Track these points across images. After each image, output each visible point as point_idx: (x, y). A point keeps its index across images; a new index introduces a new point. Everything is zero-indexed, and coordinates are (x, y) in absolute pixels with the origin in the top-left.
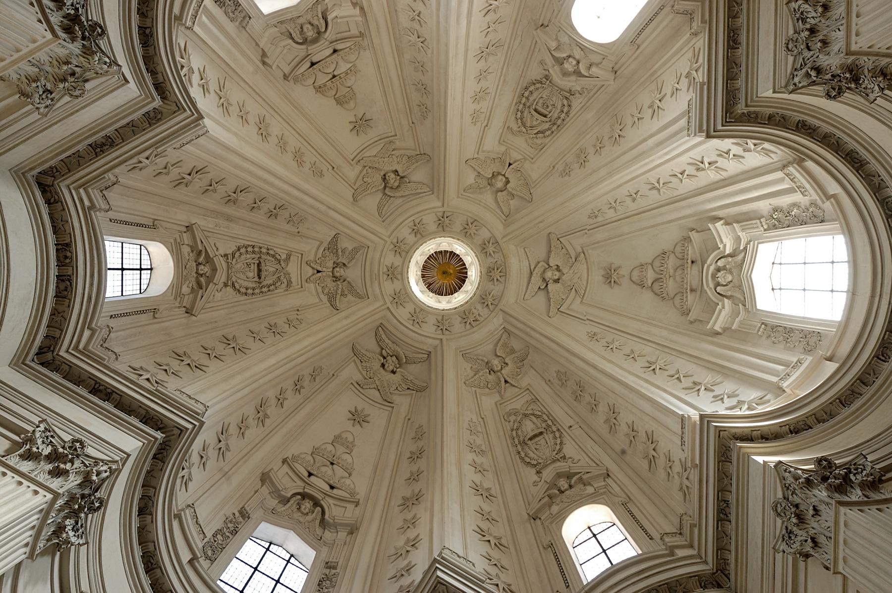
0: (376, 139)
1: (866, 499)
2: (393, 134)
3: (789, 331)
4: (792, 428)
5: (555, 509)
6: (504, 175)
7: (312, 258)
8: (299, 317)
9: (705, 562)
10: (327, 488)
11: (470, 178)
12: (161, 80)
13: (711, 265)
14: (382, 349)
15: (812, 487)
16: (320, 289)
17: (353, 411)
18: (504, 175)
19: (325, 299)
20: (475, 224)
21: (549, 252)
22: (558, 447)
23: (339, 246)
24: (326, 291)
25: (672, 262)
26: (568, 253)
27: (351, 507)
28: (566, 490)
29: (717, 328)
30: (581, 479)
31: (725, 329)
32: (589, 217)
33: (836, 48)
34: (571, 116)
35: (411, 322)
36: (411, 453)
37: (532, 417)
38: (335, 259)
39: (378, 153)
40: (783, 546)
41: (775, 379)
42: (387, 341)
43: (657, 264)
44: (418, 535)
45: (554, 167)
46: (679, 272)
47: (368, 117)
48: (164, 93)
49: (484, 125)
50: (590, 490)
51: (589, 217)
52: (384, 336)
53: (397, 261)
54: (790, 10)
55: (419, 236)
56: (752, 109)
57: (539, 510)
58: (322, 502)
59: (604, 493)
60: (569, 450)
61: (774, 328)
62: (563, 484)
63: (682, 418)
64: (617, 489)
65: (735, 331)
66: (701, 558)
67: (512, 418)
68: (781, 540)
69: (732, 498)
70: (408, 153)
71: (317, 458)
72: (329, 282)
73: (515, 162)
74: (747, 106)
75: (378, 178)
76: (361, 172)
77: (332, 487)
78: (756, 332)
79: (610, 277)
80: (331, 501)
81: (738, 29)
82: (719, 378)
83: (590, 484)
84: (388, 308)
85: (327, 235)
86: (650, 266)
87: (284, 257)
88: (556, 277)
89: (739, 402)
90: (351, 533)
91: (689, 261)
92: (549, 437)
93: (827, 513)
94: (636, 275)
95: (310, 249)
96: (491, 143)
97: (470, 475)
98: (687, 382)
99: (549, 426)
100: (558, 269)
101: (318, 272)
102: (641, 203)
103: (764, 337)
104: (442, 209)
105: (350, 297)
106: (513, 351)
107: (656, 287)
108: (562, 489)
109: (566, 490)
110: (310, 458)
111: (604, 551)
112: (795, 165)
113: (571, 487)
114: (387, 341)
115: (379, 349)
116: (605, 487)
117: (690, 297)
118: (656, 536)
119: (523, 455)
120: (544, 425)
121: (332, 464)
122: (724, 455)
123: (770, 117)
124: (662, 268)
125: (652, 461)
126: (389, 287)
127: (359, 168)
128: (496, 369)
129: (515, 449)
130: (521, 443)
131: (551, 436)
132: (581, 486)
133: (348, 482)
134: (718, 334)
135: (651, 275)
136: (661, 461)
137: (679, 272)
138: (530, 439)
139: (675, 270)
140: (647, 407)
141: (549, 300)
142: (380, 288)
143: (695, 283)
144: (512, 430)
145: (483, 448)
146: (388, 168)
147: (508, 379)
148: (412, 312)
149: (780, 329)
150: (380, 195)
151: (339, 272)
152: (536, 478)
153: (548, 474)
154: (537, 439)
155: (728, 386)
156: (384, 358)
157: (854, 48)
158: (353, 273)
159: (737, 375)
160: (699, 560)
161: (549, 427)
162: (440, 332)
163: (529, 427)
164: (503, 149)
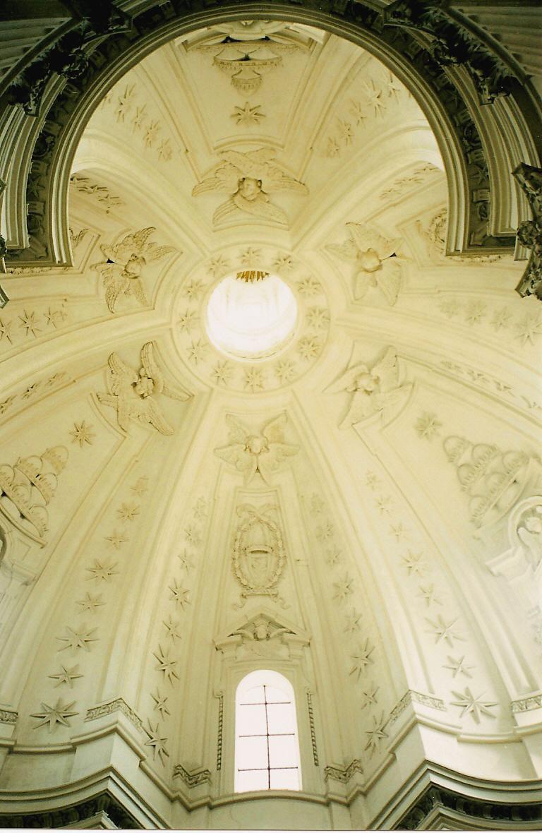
0: (257, 137)
2: (280, 143)
5: (242, 652)
6: (380, 261)
7: (107, 240)
8: (64, 310)
10: (15, 515)
11: (341, 239)
12: (39, 210)
13: (529, 503)
14: (143, 367)
16: (102, 278)
17: (79, 425)
18: (380, 261)
19: (103, 291)
20: (315, 286)
21: (380, 359)
22: (275, 579)
23: (148, 241)
24: (109, 283)
25: (494, 463)
26: (397, 374)
27: (36, 547)
28: (262, 639)
29: (494, 570)
31: (500, 574)
32: (442, 363)
34: (493, 264)
35: (189, 354)
36: (123, 505)
37: (266, 526)
38: (136, 252)
39: (250, 152)
42: (152, 361)
43: (479, 451)
44: (94, 631)
45: (439, 291)
46: (494, 479)
47: (260, 111)
48: (36, 227)
49: (393, 203)
50: (284, 652)
51: (442, 363)
52: (150, 356)
53: (207, 279)
55: (246, 264)
57: (226, 645)
58: (7, 537)
59: (294, 666)
60: (285, 588)
62: (262, 632)
67: (245, 515)
70: (286, 172)
71: (19, 473)
72: (117, 276)
73: (402, 256)
75: (235, 179)
76: (217, 165)
77: (22, 516)
79: (426, 426)
80: (16, 534)
83: (287, 644)
84: (171, 329)
85: (140, 224)
86: (471, 448)
87: (76, 233)
88: (369, 390)
90: (26, 584)
91: (512, 480)
92: (271, 559)
94: (452, 444)
95: (112, 230)
96: (388, 222)
97: (176, 572)
99: (277, 545)
100: (377, 381)
101: (109, 261)
102: (503, 395)
104: (288, 253)
105: (133, 300)
106: (280, 440)
107: (464, 472)
109: (262, 639)
110: (10, 473)
111: (269, 769)
114: (152, 361)
115: (139, 365)
116: (301, 658)
117: (490, 515)
118: (323, 765)
119: (237, 565)
120: (272, 543)
121: (33, 484)
124: (481, 461)
126: (183, 305)
127: (217, 159)
128: (254, 450)
129: (232, 551)
130: (242, 550)
131: (275, 559)
133: (42, 513)
134: (491, 573)
135: (466, 457)
137: (494, 479)
138: (252, 552)
139: (494, 473)
141: (349, 407)
142: (172, 304)
143: (505, 504)
144: (239, 529)
145: (200, 536)
146: (253, 175)
147: (260, 468)
148: (196, 341)
150: (226, 199)
151: (135, 268)
152: (238, 599)
153: (255, 605)
154: (258, 555)
156: (140, 377)
158: (149, 274)
161: (274, 550)
162: (215, 379)
163: (257, 537)
164: (398, 235)
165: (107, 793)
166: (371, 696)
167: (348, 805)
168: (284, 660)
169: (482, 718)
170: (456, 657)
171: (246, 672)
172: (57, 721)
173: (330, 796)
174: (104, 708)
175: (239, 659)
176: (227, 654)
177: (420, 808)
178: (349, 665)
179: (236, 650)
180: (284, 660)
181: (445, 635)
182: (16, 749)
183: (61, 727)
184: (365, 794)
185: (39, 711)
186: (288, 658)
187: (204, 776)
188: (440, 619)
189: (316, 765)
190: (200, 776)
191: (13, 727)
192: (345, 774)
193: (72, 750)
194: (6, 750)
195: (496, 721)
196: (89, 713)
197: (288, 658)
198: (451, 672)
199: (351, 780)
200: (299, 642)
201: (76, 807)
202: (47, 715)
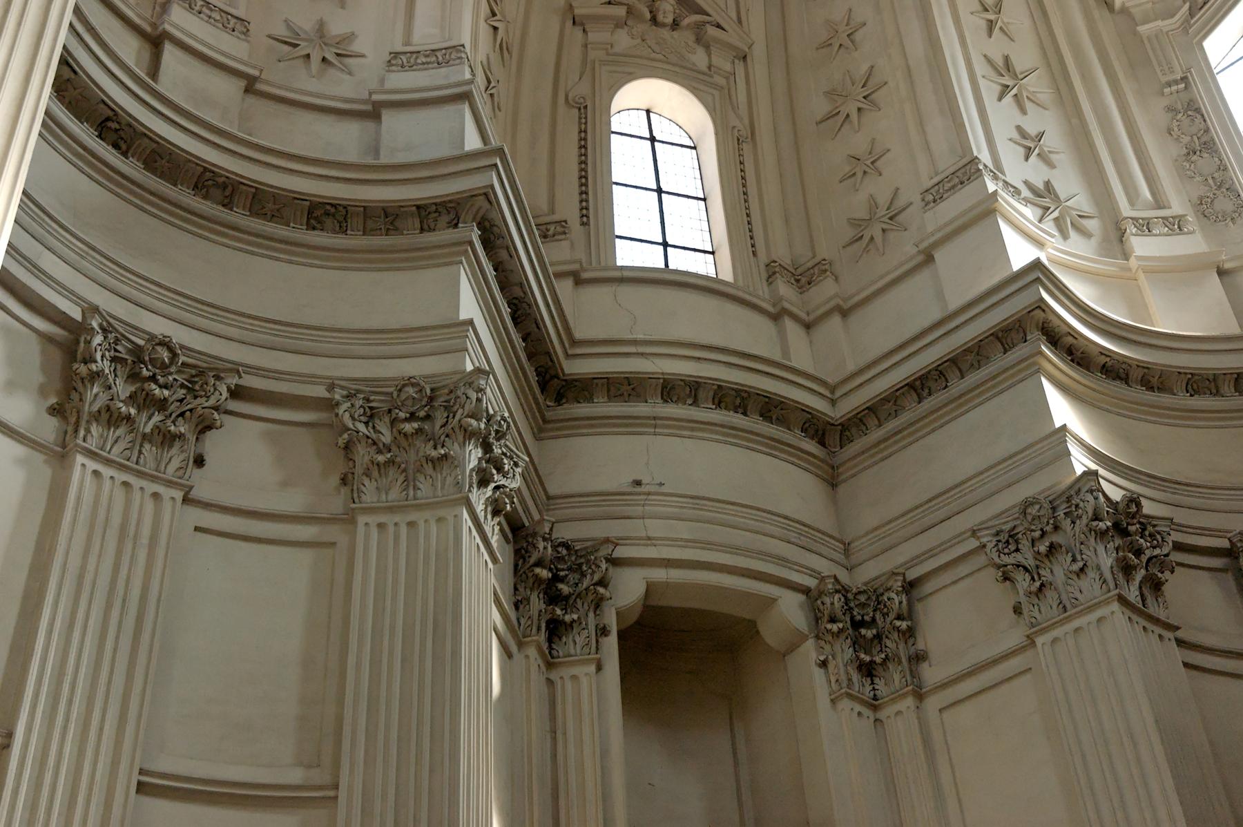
1: (1140, 606)
3: (1209, 146)
4: (1110, 364)
5: (623, 40)
9: (833, 402)
15: (1102, 539)
28: (663, 25)
30: (699, 28)
40: (987, 538)
41: (1126, 210)
50: (699, 58)
61: (1193, 109)
63: (975, 160)
64: (742, 97)
65: (1135, 33)
66: (833, 389)
68: (994, 531)
69: (958, 386)
78: (1164, 79)
82: (1045, 94)
83: (707, 47)
89: (1048, 184)
93: (1089, 587)
98: (997, 47)
103: (1165, 102)
108: (660, 18)
109: (663, 25)
113: (675, 25)
118: (763, 257)
122: (1006, 336)
125: (835, 120)
132: (689, 37)
136: (858, 142)
140: (916, 48)
149: (1199, 120)
155: (1045, 122)
159: (1075, 121)
160: (827, 393)
165: (488, 195)
166: (868, 162)
167: (808, 326)
168: (699, 72)
169: (1072, 233)
170: (1032, 131)
171: (631, 77)
172: (324, 59)
173: (787, 305)
174: (427, 56)
175: (617, 49)
176: (592, 36)
177: (998, 338)
178: (821, 107)
179: (612, 33)
180: (699, 72)
181: (1014, 91)
182: (260, 86)
183: (332, 71)
184: (845, 313)
185: (281, 31)
186: (706, 70)
187: (559, 229)
188: (1007, 59)
189: (754, 253)
190: (552, 228)
191: (245, 44)
192: (804, 278)
193: (372, 113)
194: (242, 84)
195: (1094, 241)
196: (395, 58)
197: (706, 70)
198: (1022, 151)
199: (814, 290)
200: (730, 46)
201: (418, 207)
202: (303, 44)
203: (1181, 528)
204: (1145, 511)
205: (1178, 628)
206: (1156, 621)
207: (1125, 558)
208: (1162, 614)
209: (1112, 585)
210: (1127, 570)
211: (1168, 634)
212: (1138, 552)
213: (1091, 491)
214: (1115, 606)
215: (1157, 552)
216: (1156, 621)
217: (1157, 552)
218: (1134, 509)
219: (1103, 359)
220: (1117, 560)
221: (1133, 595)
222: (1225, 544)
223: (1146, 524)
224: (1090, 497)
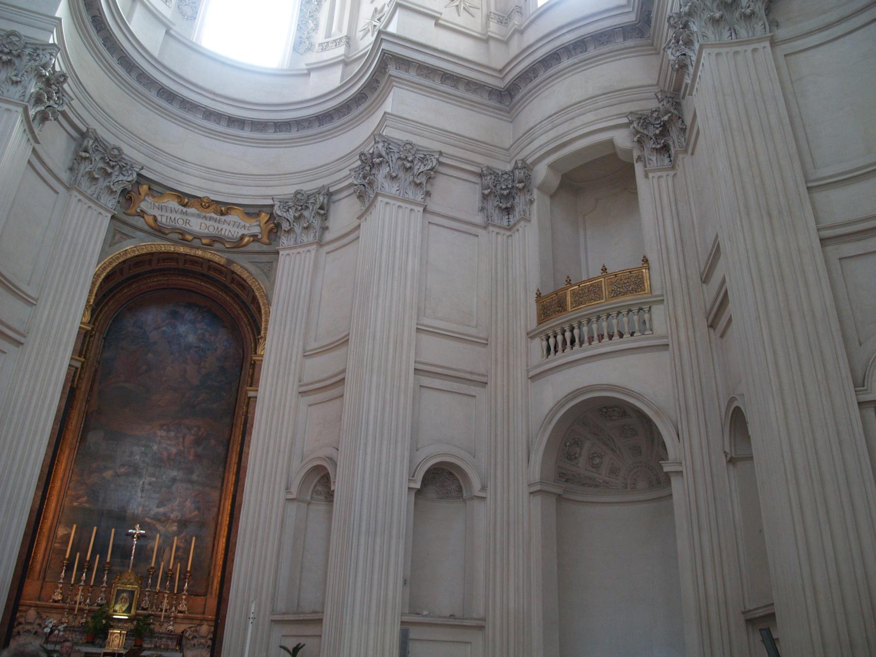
33: (386, 185)
54: (435, 152)
56: (387, 76)
74: (390, 76)
81: (455, 86)
112: (343, 58)
123: (378, 82)
157: (380, 198)
203: (71, 107)
204: (65, 86)
205: (38, 143)
206: (32, 132)
207: (42, 94)
208: (36, 131)
209: (27, 99)
210: (38, 100)
211: (32, 141)
212: (49, 98)
213: (51, 54)
214: (20, 110)
215: (56, 106)
216: (32, 132)
217: (56, 106)
218: (62, 79)
219: (97, 13)
220: (37, 92)
221: (32, 112)
222: (84, 129)
223: (60, 92)
224: (48, 57)
